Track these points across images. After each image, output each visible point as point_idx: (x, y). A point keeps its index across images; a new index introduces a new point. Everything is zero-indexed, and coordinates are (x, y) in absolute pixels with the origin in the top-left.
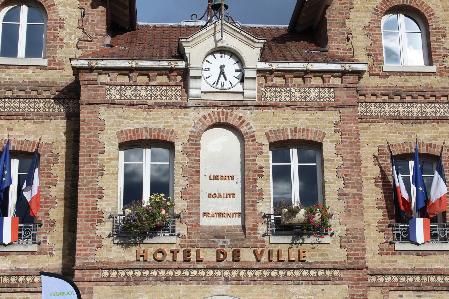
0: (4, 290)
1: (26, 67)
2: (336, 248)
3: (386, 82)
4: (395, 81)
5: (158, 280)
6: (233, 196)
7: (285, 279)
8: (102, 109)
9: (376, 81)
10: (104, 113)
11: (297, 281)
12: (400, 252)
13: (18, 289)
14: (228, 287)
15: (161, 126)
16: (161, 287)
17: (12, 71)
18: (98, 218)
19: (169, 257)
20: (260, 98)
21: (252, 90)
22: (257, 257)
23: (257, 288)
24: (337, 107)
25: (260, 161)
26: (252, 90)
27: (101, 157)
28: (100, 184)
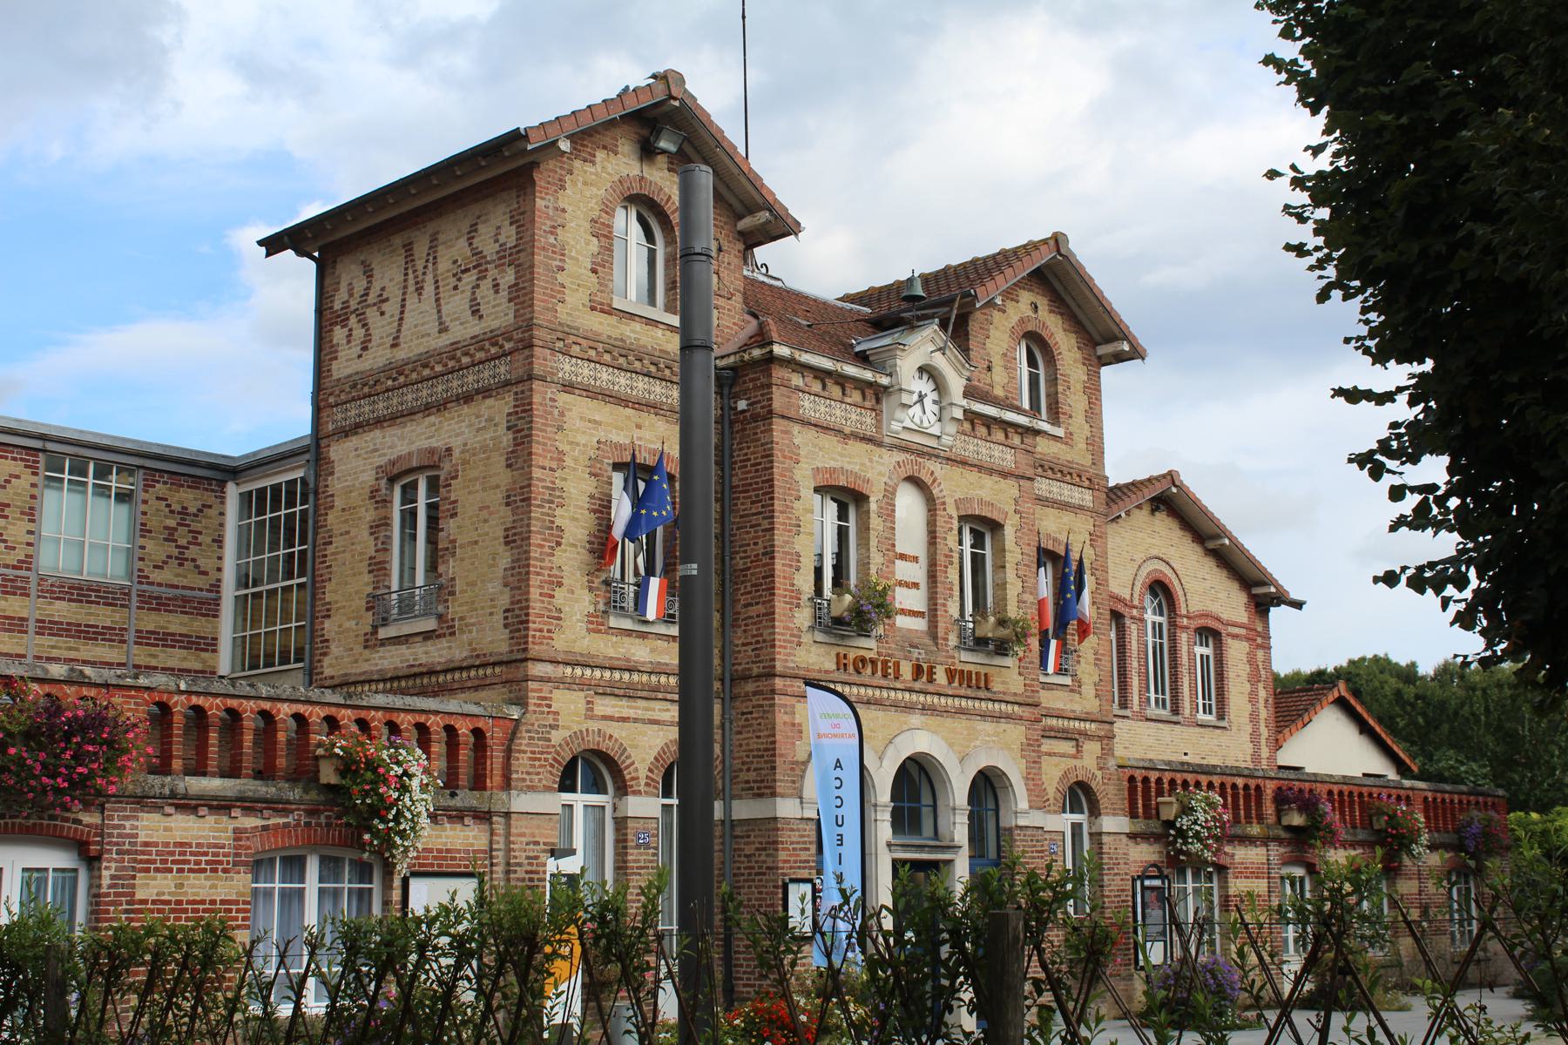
0: (644, 694)
6: (916, 585)
8: (796, 428)
10: (802, 437)
11: (984, 716)
13: (660, 696)
14: (923, 718)
15: (856, 468)
17: (637, 326)
21: (951, 438)
23: (948, 722)
26: (951, 438)
27: (797, 504)
28: (798, 548)
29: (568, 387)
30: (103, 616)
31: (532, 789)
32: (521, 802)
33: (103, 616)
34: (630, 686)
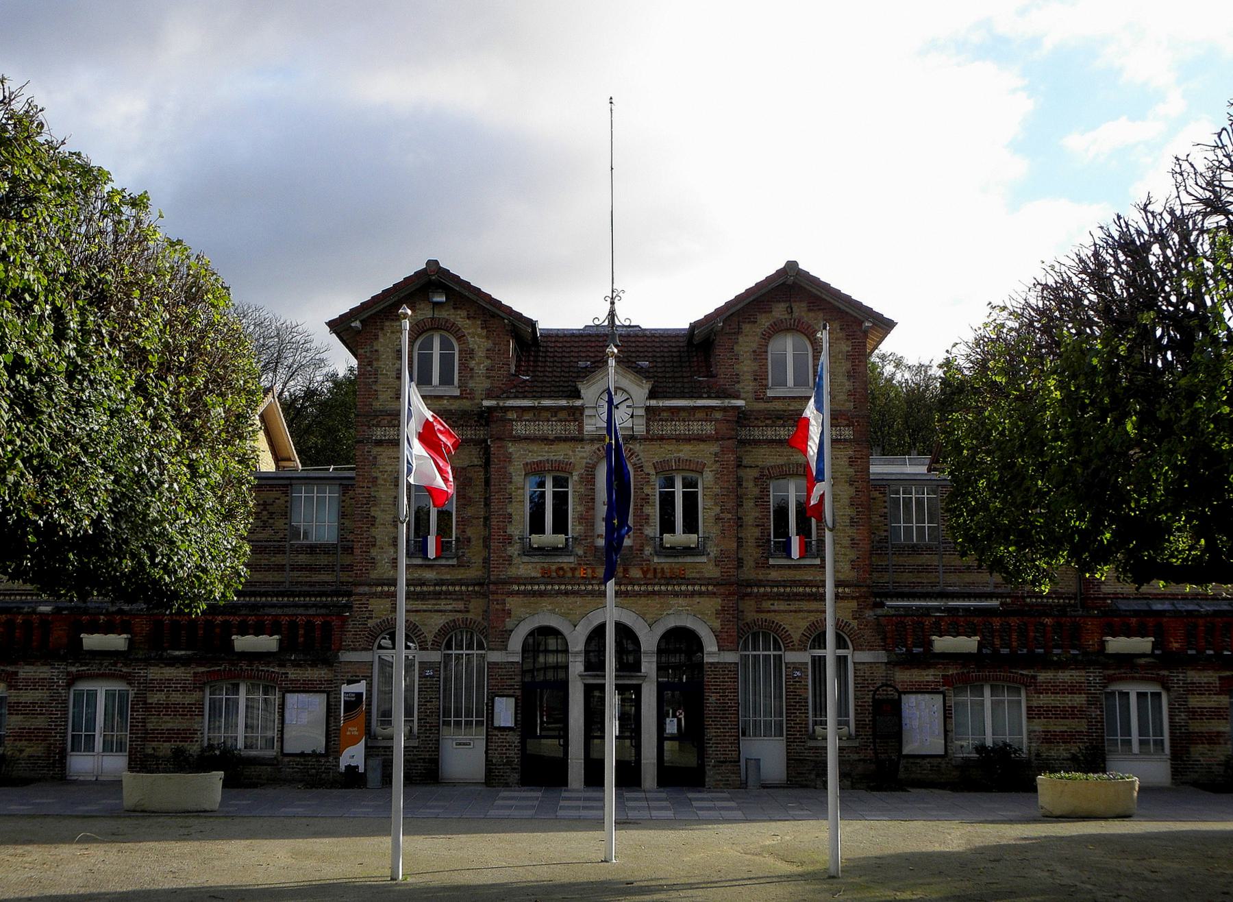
1: (441, 397)
2: (711, 567)
3: (768, 406)
4: (778, 406)
5: (559, 592)
7: (667, 593)
9: (761, 406)
10: (512, 448)
11: (676, 595)
12: (773, 566)
16: (561, 599)
18: (509, 540)
19: (570, 575)
20: (648, 431)
22: (645, 573)
23: (643, 600)
24: (717, 440)
25: (647, 490)
29: (379, 443)
30: (323, 560)
31: (354, 649)
32: (347, 656)
33: (323, 560)
34: (422, 593)
